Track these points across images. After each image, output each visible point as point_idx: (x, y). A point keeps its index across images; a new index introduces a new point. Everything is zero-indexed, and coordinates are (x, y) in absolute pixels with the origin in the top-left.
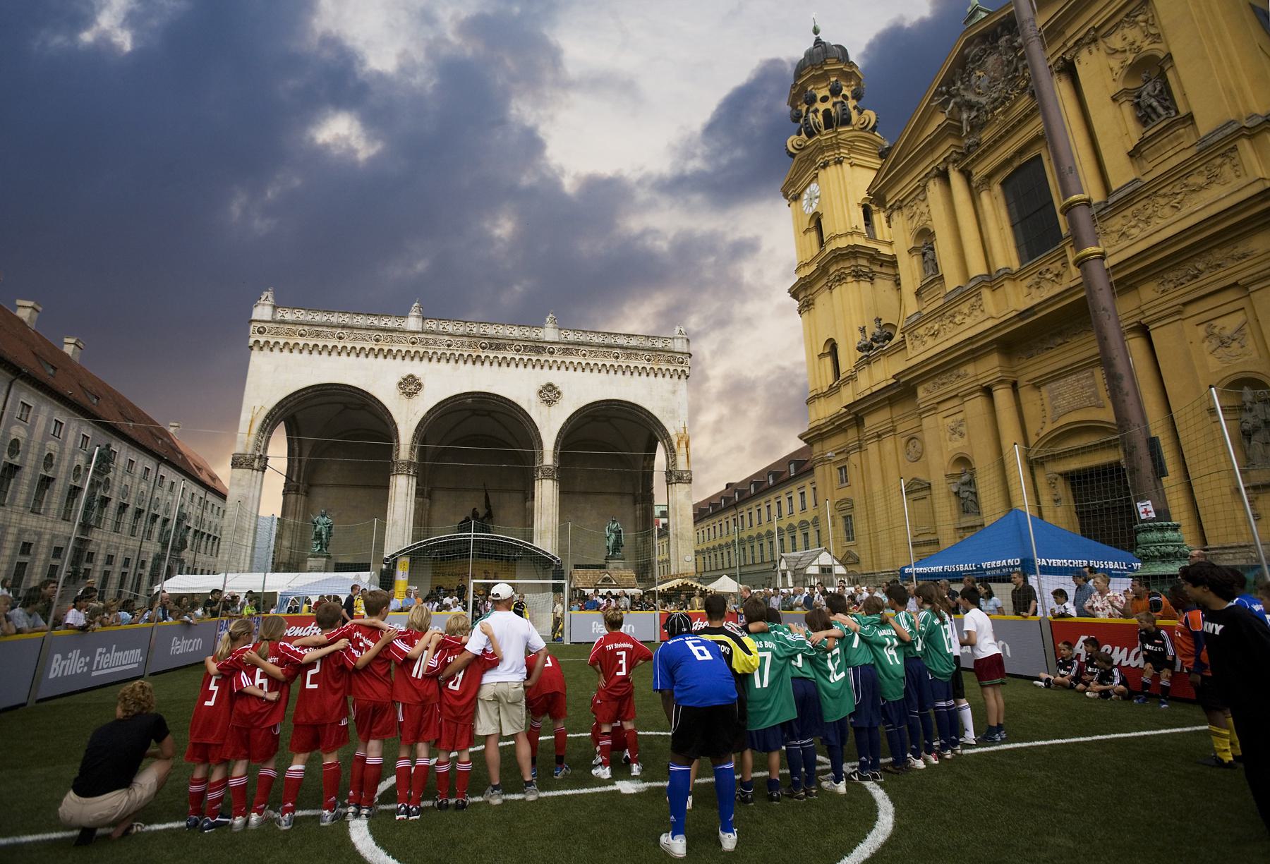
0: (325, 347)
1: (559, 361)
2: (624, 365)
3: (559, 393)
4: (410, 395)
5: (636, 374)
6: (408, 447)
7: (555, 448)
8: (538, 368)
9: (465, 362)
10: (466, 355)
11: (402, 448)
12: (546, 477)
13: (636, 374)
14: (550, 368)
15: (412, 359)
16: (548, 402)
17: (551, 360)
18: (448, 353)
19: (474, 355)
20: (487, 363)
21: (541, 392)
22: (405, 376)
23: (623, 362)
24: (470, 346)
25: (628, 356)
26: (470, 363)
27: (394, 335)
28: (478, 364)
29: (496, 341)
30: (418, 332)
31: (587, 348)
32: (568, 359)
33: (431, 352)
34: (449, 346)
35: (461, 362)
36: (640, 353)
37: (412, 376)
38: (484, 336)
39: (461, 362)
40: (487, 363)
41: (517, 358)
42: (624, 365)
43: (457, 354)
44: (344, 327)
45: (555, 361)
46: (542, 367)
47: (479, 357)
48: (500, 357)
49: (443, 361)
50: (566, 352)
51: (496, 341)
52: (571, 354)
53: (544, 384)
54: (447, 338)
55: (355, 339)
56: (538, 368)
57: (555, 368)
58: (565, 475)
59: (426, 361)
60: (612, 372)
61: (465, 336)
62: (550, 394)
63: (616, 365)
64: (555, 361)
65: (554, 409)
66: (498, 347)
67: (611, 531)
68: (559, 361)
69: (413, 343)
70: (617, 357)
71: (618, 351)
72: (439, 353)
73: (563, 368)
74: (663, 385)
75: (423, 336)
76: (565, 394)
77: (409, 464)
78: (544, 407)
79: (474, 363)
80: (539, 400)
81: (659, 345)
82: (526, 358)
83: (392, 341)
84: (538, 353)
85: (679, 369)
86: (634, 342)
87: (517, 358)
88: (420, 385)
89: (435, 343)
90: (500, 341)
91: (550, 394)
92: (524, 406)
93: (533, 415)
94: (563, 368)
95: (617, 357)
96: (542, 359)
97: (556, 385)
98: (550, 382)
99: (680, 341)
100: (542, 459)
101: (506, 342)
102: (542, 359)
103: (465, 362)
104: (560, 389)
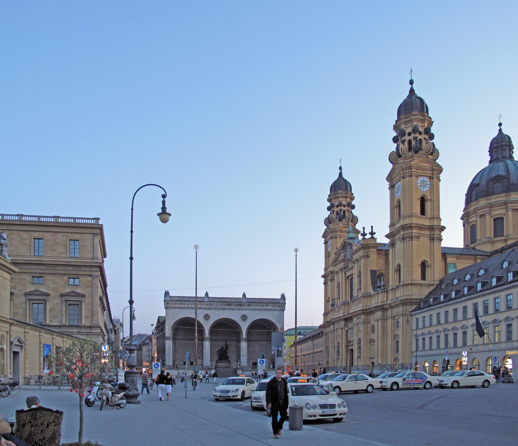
0: (184, 307)
1: (247, 308)
2: (265, 308)
3: (247, 317)
4: (207, 319)
5: (269, 311)
6: (208, 334)
7: (246, 332)
8: (241, 311)
9: (221, 310)
10: (221, 307)
11: (206, 334)
12: (244, 341)
13: (269, 311)
14: (244, 310)
15: (207, 309)
16: (244, 320)
17: (244, 308)
18: (216, 307)
19: (223, 307)
20: (227, 310)
21: (242, 317)
22: (205, 314)
23: (265, 307)
24: (222, 305)
25: (266, 306)
26: (222, 310)
27: (202, 303)
28: (224, 310)
29: (229, 303)
30: (208, 302)
31: (255, 304)
32: (249, 307)
33: (212, 307)
34: (216, 305)
35: (220, 310)
36: (270, 304)
37: (207, 314)
38: (226, 302)
39: (220, 310)
40: (227, 310)
41: (235, 308)
42: (265, 308)
43: (219, 307)
44: (188, 301)
45: (245, 308)
46: (242, 310)
47: (224, 308)
48: (230, 308)
49: (215, 310)
50: (249, 305)
51: (229, 303)
52: (250, 306)
53: (243, 315)
54: (216, 303)
55: (191, 304)
56: (241, 311)
57: (245, 310)
58: (248, 340)
59: (210, 310)
60: (262, 311)
61: (220, 302)
62: (244, 318)
63: (263, 308)
64: (245, 308)
65: (246, 322)
66: (230, 305)
67: (261, 355)
68: (247, 308)
69: (207, 305)
70: (263, 306)
71: (264, 304)
72: (214, 307)
73: (248, 310)
74: (277, 313)
75: (209, 303)
76: (249, 317)
77: (208, 338)
78: (243, 322)
79: (223, 310)
80: (241, 320)
81: (276, 301)
82: (237, 308)
83: (201, 305)
84: (241, 306)
85: (282, 309)
86: (268, 301)
87: (235, 308)
88: (209, 317)
89: (213, 305)
90: (230, 303)
91: (244, 318)
92: (237, 321)
93: (240, 324)
94: (248, 310)
95: (263, 306)
96: (242, 308)
97: (246, 315)
98: (244, 314)
99: (282, 300)
100: (242, 336)
101: (231, 303)
102: (242, 308)
103: (221, 310)
104: (247, 316)
